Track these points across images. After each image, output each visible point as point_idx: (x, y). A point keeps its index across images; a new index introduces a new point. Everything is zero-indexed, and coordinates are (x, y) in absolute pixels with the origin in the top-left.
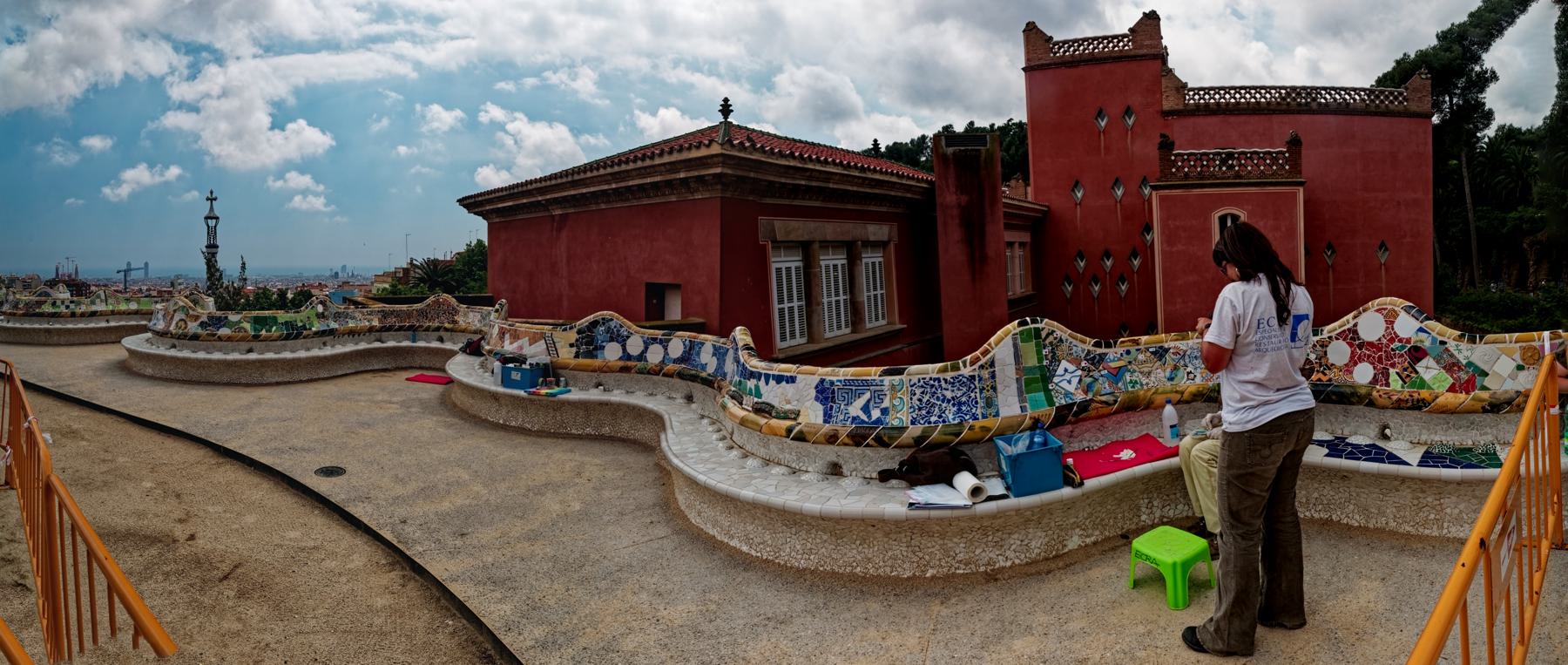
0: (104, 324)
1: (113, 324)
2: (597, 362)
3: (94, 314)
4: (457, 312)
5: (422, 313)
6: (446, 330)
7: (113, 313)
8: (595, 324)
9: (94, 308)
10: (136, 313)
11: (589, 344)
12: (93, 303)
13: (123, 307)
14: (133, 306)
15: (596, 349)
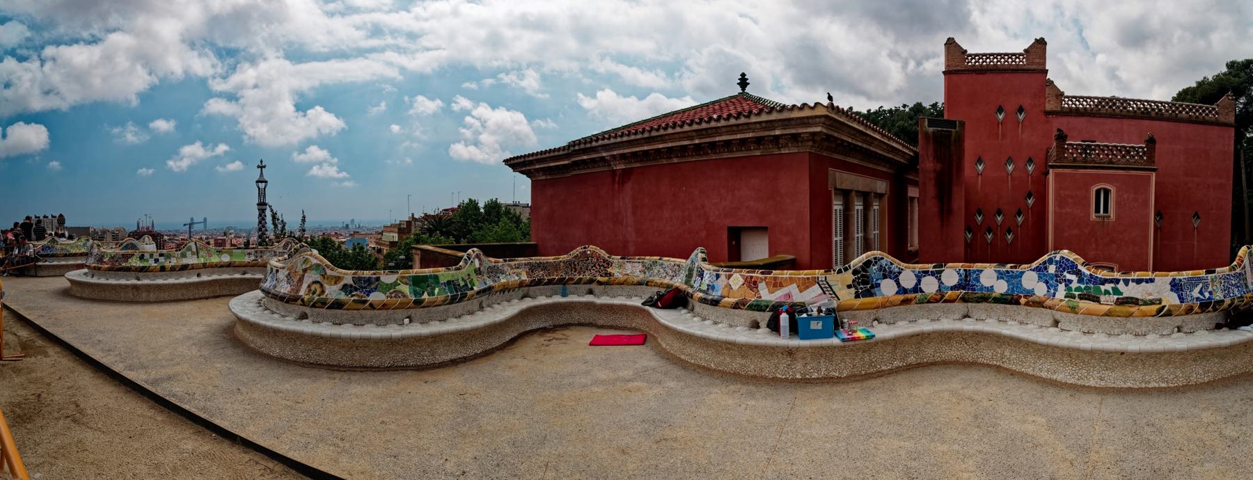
0: (195, 279)
1: (205, 278)
2: (878, 299)
3: (184, 268)
4: (609, 264)
5: (570, 265)
6: (600, 283)
7: (205, 266)
8: (868, 264)
9: (185, 261)
10: (229, 265)
11: (865, 283)
12: (184, 256)
13: (215, 259)
14: (226, 259)
15: (872, 287)
